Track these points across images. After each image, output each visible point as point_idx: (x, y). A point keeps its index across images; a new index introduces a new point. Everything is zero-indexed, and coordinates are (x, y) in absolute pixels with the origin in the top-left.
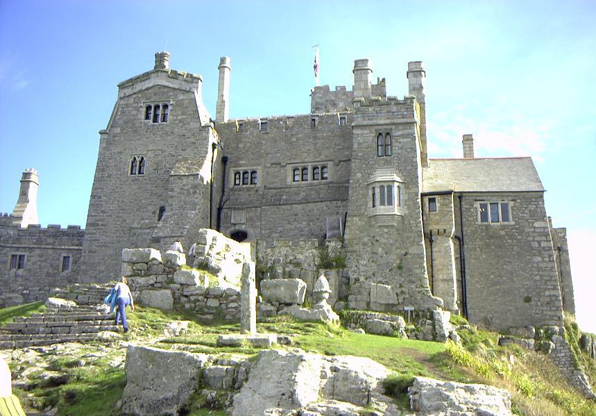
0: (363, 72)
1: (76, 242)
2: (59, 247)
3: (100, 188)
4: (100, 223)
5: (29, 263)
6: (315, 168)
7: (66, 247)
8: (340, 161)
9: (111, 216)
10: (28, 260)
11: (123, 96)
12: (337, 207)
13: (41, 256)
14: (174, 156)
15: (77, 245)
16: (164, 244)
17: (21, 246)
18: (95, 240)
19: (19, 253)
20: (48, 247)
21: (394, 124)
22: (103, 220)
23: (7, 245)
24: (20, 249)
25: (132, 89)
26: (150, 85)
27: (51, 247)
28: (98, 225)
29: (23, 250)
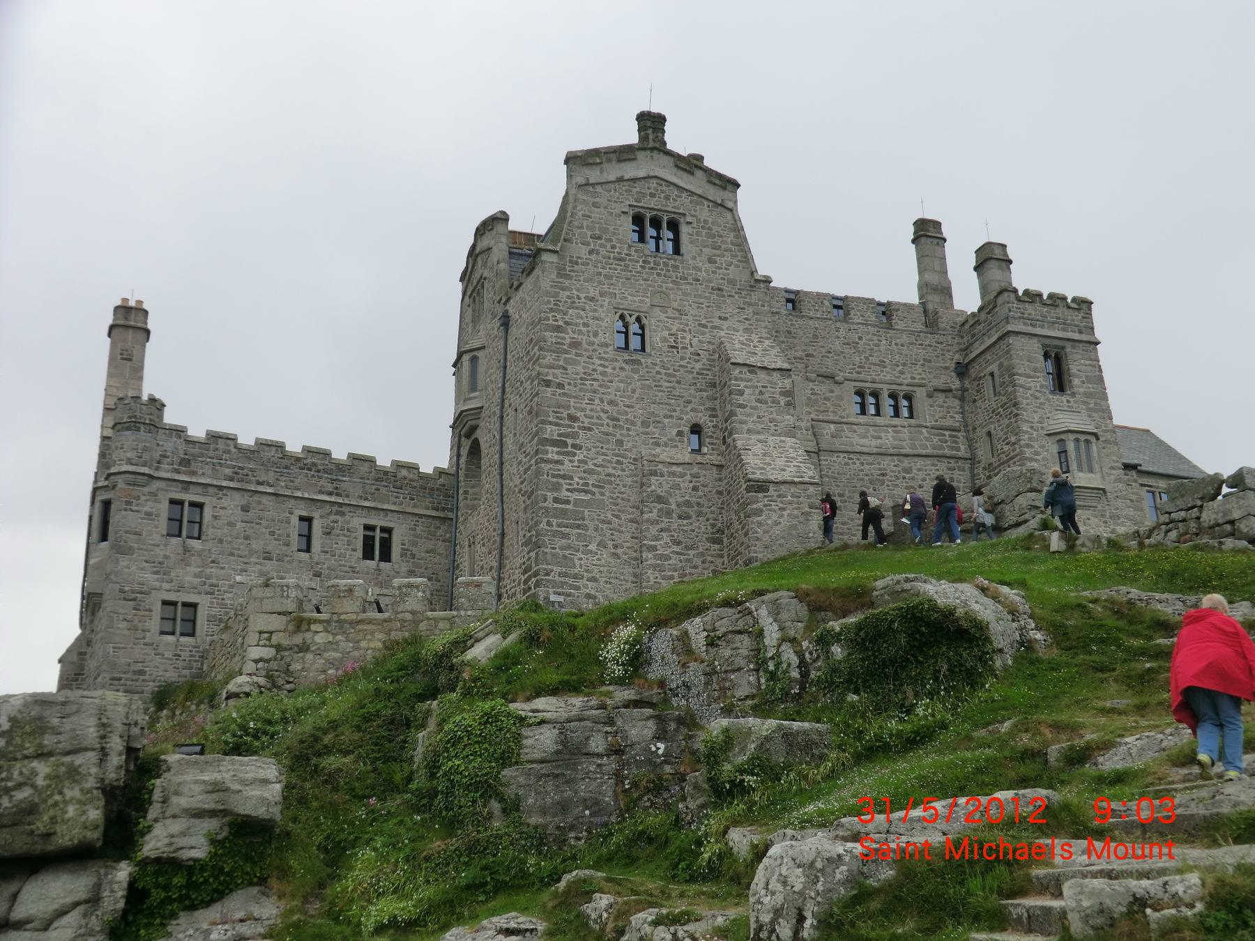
0: (935, 241)
1: (329, 487)
3: (559, 367)
4: (570, 441)
5: (217, 523)
7: (306, 495)
8: (935, 390)
9: (590, 429)
10: (216, 517)
11: (581, 180)
12: (949, 469)
13: (245, 509)
14: (705, 326)
15: (330, 494)
16: (779, 496)
17: (194, 480)
18: (564, 477)
19: (187, 497)
20: (261, 488)
22: (574, 436)
23: (156, 475)
25: (601, 172)
26: (642, 174)
27: (270, 490)
28: (565, 444)
29: (200, 489)
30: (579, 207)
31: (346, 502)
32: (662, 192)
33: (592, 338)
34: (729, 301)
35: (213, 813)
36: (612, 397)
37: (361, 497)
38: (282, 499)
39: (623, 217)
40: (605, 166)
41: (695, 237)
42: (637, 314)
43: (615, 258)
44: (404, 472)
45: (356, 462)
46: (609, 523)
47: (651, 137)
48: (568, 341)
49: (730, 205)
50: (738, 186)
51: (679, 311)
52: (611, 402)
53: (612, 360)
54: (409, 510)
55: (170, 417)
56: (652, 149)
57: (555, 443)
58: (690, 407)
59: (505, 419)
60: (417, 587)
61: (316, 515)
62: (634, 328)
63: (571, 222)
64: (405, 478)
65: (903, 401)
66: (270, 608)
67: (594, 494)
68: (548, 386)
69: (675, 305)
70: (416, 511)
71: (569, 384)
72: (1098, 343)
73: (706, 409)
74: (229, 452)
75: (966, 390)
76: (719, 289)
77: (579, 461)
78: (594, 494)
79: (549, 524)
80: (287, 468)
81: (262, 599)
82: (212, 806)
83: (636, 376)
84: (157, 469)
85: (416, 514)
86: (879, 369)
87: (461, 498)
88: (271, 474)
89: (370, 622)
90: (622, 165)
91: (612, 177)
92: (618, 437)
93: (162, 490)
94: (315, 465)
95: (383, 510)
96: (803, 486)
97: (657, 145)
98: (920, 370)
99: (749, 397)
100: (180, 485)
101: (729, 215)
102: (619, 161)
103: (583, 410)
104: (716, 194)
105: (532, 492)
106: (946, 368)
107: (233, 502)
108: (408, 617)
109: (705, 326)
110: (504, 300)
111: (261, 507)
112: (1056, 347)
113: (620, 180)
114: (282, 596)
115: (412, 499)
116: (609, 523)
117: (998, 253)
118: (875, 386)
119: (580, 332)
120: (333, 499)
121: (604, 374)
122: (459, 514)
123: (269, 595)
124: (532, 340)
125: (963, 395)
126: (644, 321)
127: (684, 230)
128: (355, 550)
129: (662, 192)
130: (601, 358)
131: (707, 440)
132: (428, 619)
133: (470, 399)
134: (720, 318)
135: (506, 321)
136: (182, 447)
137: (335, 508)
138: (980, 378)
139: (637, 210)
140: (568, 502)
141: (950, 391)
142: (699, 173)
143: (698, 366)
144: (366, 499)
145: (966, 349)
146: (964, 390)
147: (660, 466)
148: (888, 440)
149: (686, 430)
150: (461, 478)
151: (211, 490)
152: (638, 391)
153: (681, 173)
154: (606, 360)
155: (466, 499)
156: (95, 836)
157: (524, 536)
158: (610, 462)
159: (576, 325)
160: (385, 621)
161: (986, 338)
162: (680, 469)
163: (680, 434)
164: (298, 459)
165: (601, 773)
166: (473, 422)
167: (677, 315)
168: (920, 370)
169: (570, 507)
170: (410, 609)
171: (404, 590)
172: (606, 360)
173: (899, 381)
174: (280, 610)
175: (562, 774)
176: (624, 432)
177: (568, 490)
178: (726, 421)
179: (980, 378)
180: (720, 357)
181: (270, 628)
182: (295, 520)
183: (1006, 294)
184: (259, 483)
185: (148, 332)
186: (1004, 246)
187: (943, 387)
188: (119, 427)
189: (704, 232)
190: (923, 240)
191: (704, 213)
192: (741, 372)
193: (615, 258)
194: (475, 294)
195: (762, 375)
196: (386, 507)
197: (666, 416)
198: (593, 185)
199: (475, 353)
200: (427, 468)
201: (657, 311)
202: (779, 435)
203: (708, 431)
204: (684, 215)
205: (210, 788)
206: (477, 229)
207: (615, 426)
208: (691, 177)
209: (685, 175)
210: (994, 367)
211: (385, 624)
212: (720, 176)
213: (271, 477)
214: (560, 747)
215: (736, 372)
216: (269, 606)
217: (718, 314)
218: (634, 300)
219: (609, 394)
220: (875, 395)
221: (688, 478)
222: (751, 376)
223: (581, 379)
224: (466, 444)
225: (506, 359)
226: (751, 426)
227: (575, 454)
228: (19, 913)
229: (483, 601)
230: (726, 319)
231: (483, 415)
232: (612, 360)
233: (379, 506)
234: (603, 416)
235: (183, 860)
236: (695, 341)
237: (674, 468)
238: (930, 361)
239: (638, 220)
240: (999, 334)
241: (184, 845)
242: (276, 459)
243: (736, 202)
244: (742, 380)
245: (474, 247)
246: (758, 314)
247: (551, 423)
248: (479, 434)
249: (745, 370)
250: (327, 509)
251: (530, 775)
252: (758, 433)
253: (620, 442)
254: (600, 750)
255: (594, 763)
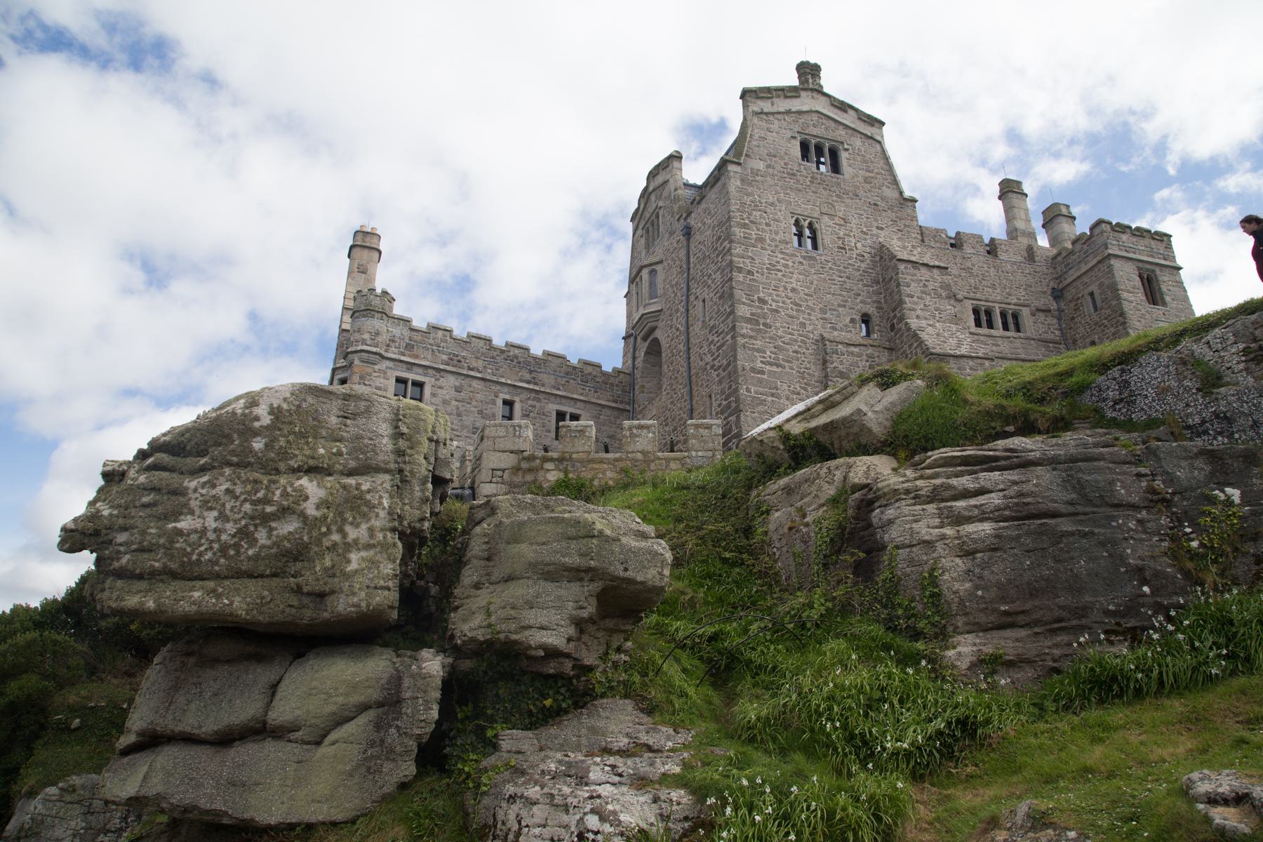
1: (528, 376)
2: (495, 378)
4: (762, 321)
6: (1003, 315)
7: (509, 382)
9: (777, 311)
13: (458, 390)
15: (528, 382)
18: (758, 350)
19: (411, 376)
21: (1157, 264)
24: (415, 369)
25: (773, 105)
26: (805, 108)
27: (479, 375)
28: (758, 323)
29: (420, 370)
30: (756, 131)
31: (542, 389)
32: (823, 124)
33: (774, 236)
34: (884, 214)
35: (577, 574)
36: (794, 285)
37: (554, 388)
38: (488, 383)
39: (793, 141)
40: (775, 100)
41: (851, 161)
42: (809, 220)
43: (788, 173)
44: (589, 369)
45: (550, 358)
46: (798, 394)
47: (810, 81)
48: (754, 236)
49: (878, 138)
50: (883, 124)
51: (844, 219)
52: (793, 290)
53: (792, 255)
54: (594, 400)
55: (398, 310)
56: (812, 90)
57: (748, 321)
58: (860, 298)
59: (691, 312)
60: (647, 427)
61: (517, 399)
62: (807, 232)
63: (750, 142)
64: (590, 374)
65: (1012, 321)
66: (502, 446)
67: (783, 367)
68: (740, 272)
69: (841, 214)
70: (599, 402)
71: (757, 272)
72: (1180, 268)
73: (873, 302)
74: (446, 341)
75: (1063, 311)
76: (875, 205)
77: (770, 338)
78: (783, 367)
79: (748, 390)
80: (493, 358)
81: (495, 438)
82: (573, 560)
83: (813, 271)
84: (386, 351)
85: (600, 405)
86: (991, 290)
87: (637, 392)
88: (480, 362)
89: (601, 461)
90: (788, 101)
91: (782, 110)
92: (801, 320)
93: (391, 368)
94: (517, 357)
95: (573, 399)
96: (979, 361)
97: (817, 87)
98: (1023, 293)
99: (914, 288)
100: (404, 366)
101: (878, 147)
102: (786, 97)
103: (770, 295)
104: (868, 130)
105: (729, 364)
106: (1044, 293)
107: (452, 381)
108: (640, 456)
109: (867, 234)
110: (684, 216)
111: (472, 389)
112: (1148, 270)
113: (789, 112)
114: (515, 436)
115: (596, 392)
116: (798, 394)
117: (1064, 211)
118: (988, 304)
119: (763, 230)
120: (531, 386)
121: (786, 266)
122: (636, 406)
123: (501, 434)
124: (720, 238)
125: (1060, 315)
126: (816, 226)
127: (844, 156)
128: (549, 431)
129: (823, 124)
130: (782, 253)
131: (876, 328)
132: (659, 459)
133: (650, 304)
134: (878, 228)
135: (688, 232)
136: (406, 333)
137: (533, 395)
138: (1078, 299)
139: (804, 136)
140: (763, 373)
141: (1050, 311)
142: (851, 112)
143: (863, 266)
144: (559, 389)
145: (1061, 276)
146: (1060, 310)
147: (840, 346)
148: (1005, 348)
149: (858, 318)
150: (638, 374)
151: (430, 371)
152: (815, 282)
153: (836, 110)
154: (787, 254)
155: (643, 392)
156: (387, 598)
157: (719, 405)
158: (796, 341)
159: (760, 224)
160: (616, 460)
161: (1083, 265)
162: (856, 350)
163: (852, 321)
164: (502, 352)
165: (1145, 532)
166: (653, 324)
167: (842, 222)
168: (1023, 293)
169: (765, 377)
170: (640, 448)
171: (635, 431)
172: (787, 254)
173: (1007, 301)
174: (512, 448)
175: (1093, 533)
176: (806, 316)
177: (762, 362)
178: (894, 310)
179: (1078, 299)
180: (881, 258)
181: (503, 466)
182: (499, 402)
183: (1103, 225)
184: (470, 369)
185: (380, 252)
186: (1068, 207)
187: (1043, 308)
188: (357, 314)
189: (859, 158)
190: (1010, 195)
191: (858, 142)
192: (906, 268)
193: (788, 173)
194: (648, 225)
195: (924, 270)
196: (575, 396)
197: (839, 306)
198: (767, 114)
199: (654, 267)
200: (607, 368)
201: (826, 218)
202: (944, 322)
203: (875, 320)
204: (842, 143)
205: (572, 531)
206: (650, 172)
207: (798, 311)
208: (845, 115)
209: (840, 113)
210: (1094, 288)
211: (617, 463)
212: (869, 116)
213: (480, 364)
214: (1074, 496)
215: (902, 267)
216: (501, 445)
217: (875, 224)
218: (808, 208)
219: (791, 283)
220: (988, 313)
221: (865, 357)
222: (915, 272)
223: (767, 269)
224: (643, 347)
225: (689, 262)
226: (919, 312)
227: (766, 332)
228: (282, 712)
229: (713, 443)
230: (882, 229)
231: (661, 317)
232: (792, 255)
233: (570, 395)
234: (789, 301)
235: (530, 647)
236: (859, 245)
237: (852, 349)
238: (1031, 286)
239: (804, 146)
240: (1099, 258)
241: (532, 622)
242: (485, 351)
243: (882, 137)
244: (907, 274)
245: (646, 189)
246: (908, 226)
247: (744, 303)
248: (658, 334)
249: (910, 266)
250: (525, 395)
251: (1041, 534)
252: (926, 319)
253: (803, 325)
254: (1135, 499)
255: (1133, 516)
